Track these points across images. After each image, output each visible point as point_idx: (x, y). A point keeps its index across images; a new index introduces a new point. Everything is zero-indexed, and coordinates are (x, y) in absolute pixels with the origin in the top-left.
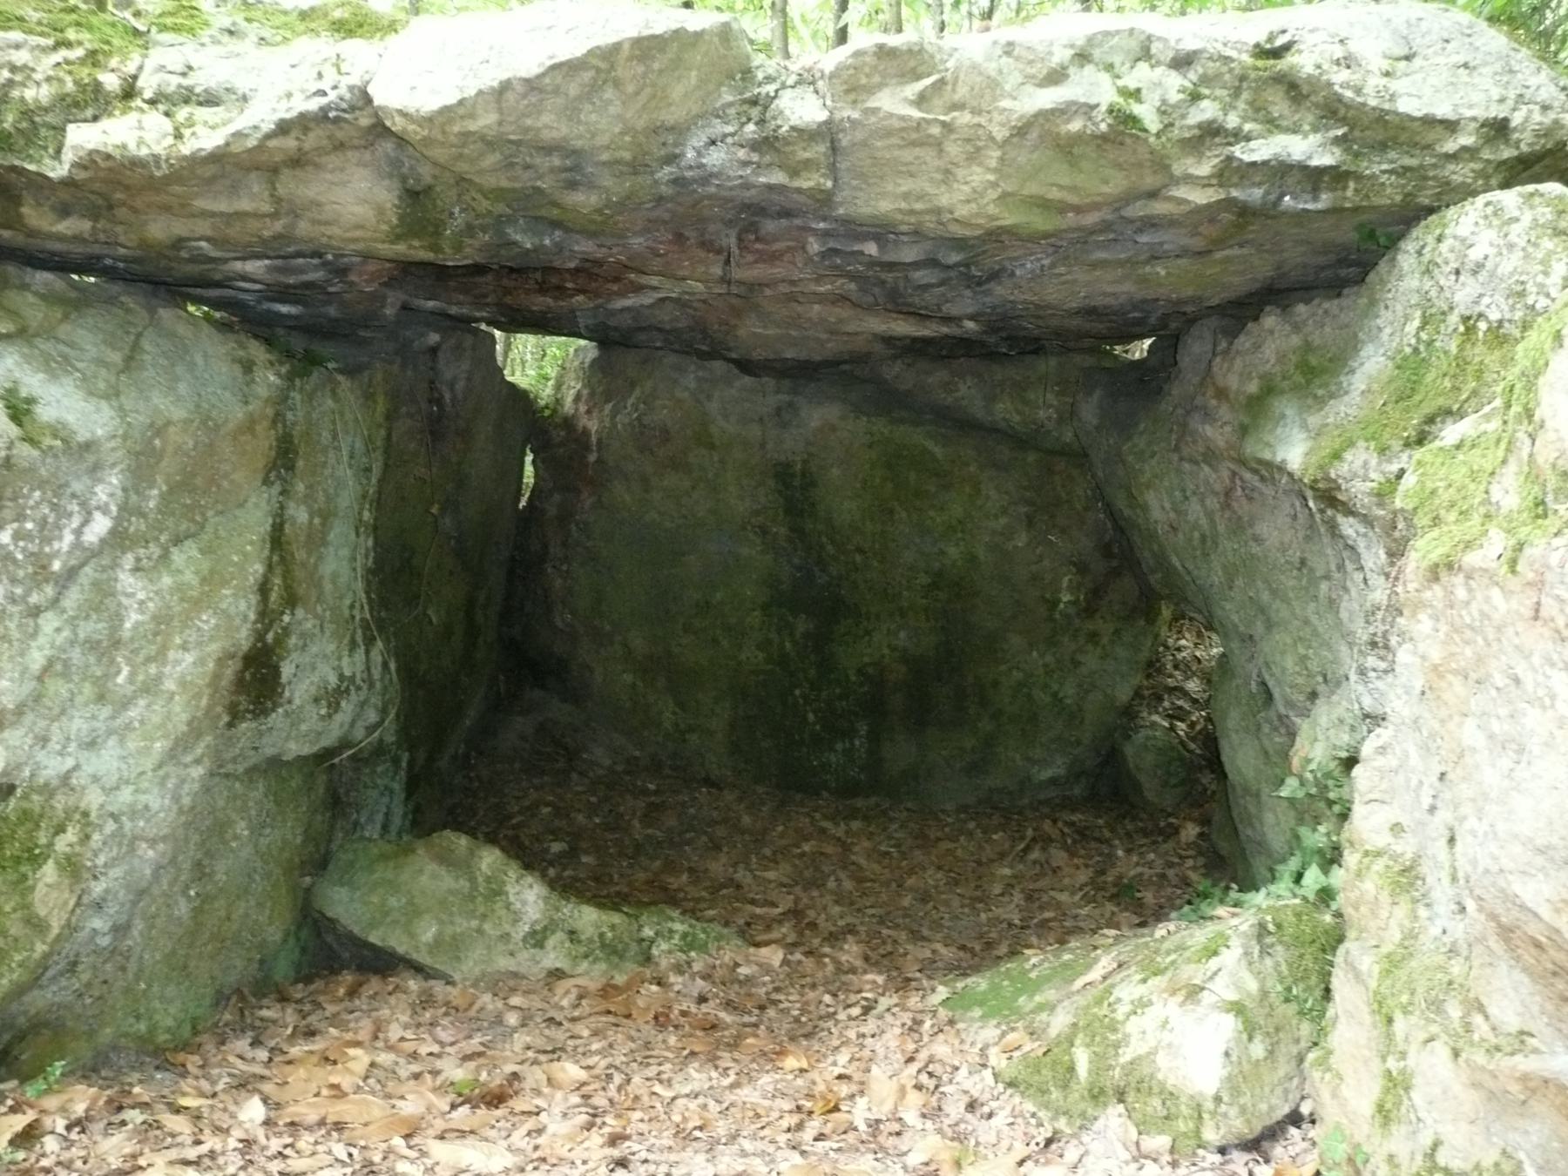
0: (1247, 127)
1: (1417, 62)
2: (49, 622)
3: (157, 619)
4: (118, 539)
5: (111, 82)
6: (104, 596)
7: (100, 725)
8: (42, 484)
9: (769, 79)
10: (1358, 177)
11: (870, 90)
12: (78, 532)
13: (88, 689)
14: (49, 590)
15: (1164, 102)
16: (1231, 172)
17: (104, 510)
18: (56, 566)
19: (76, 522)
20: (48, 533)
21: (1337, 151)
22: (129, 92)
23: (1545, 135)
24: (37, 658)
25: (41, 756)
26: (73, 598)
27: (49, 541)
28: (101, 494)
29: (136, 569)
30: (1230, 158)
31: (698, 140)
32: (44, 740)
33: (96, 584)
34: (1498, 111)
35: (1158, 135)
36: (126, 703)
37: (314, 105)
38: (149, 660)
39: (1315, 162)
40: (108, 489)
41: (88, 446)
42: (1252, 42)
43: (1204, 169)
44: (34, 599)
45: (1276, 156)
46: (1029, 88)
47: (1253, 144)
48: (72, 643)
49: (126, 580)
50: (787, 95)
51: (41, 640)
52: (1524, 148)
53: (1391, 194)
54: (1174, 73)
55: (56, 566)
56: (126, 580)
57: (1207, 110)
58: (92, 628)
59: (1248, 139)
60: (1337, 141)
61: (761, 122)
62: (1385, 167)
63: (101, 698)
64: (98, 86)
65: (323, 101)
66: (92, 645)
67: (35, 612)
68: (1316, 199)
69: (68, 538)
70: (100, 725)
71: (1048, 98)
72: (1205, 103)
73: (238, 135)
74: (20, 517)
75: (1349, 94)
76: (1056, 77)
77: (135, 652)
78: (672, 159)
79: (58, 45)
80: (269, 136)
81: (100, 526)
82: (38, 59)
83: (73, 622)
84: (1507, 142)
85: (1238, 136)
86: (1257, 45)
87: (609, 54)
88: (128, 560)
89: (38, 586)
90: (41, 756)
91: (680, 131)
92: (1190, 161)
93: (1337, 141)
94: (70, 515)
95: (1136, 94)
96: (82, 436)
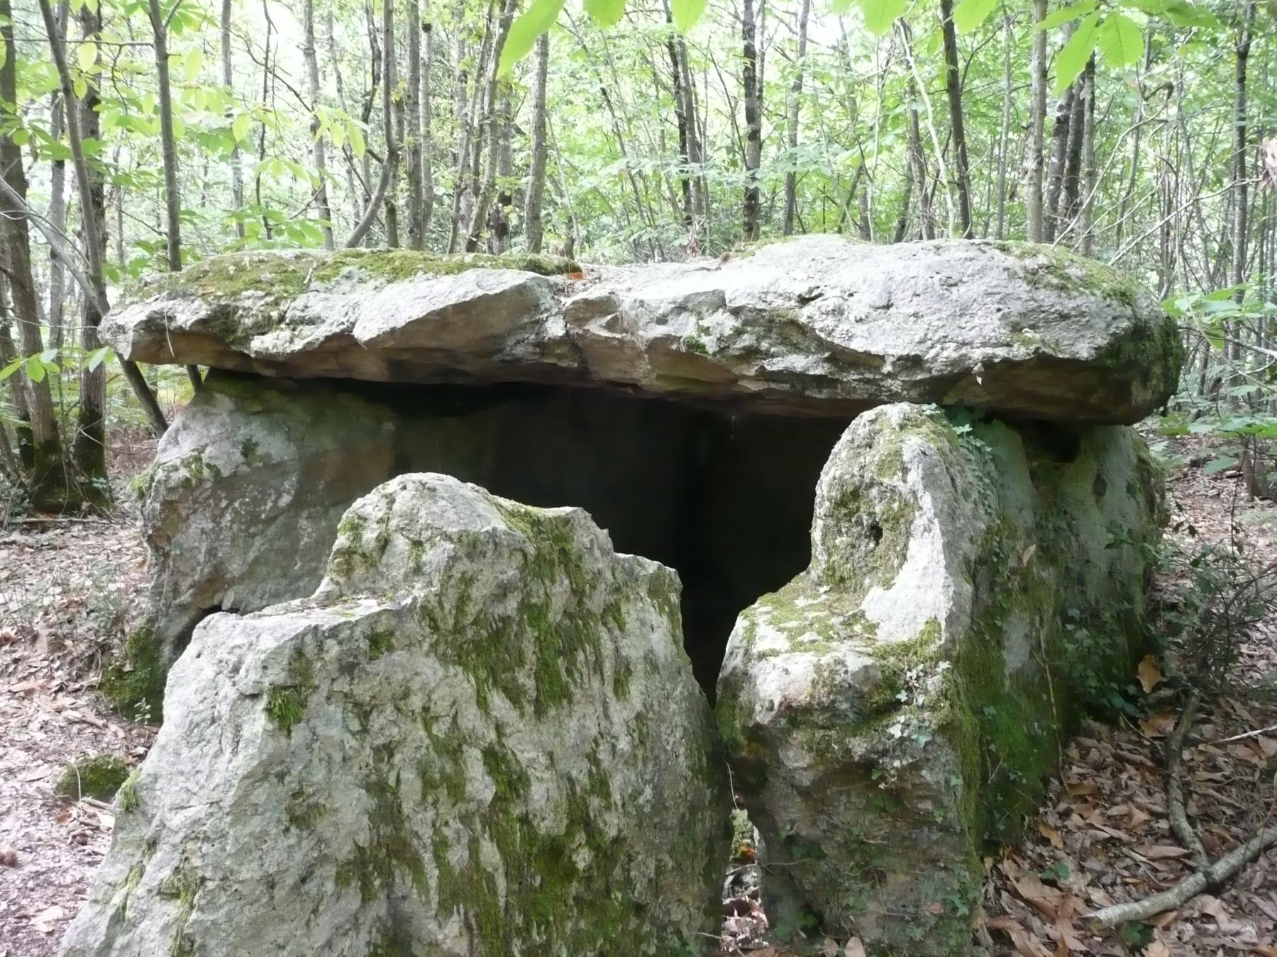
0: (773, 349)
1: (892, 310)
2: (258, 541)
3: (317, 541)
4: (298, 504)
5: (275, 314)
6: (290, 531)
7: (282, 588)
8: (254, 483)
9: (547, 310)
10: (842, 382)
11: (587, 320)
12: (275, 502)
13: (278, 571)
14: (260, 527)
15: (722, 335)
16: (764, 375)
17: (288, 493)
18: (263, 516)
19: (273, 498)
20: (257, 502)
21: (826, 365)
22: (282, 319)
23: (952, 365)
24: (251, 556)
25: (251, 598)
26: (272, 530)
27: (259, 506)
28: (287, 485)
29: (307, 518)
30: (762, 367)
31: (510, 342)
32: (254, 592)
33: (284, 525)
34: (913, 351)
35: (714, 354)
36: (298, 578)
37: (337, 330)
38: (312, 560)
39: (811, 373)
40: (290, 483)
41: (279, 465)
42: (797, 293)
43: (752, 372)
44: (252, 530)
45: (786, 369)
46: (653, 325)
47: (775, 360)
48: (271, 550)
49: (303, 523)
50: (551, 319)
51: (254, 548)
52: (934, 373)
53: (861, 393)
54: (732, 317)
55: (263, 516)
56: (303, 523)
57: (747, 340)
58: (283, 543)
59: (773, 356)
60: (827, 360)
61: (538, 334)
62: (856, 377)
63: (284, 576)
64: (270, 317)
65: (342, 327)
66: (280, 552)
67: (253, 536)
68: (820, 392)
69: (270, 504)
70: (282, 588)
71: (659, 331)
72: (746, 336)
73: (309, 343)
74: (244, 496)
75: (823, 335)
76: (662, 321)
77: (305, 556)
78: (500, 351)
79: (267, 295)
80: (322, 343)
81: (286, 500)
82: (254, 304)
83: (271, 541)
84: (922, 369)
85: (768, 355)
86: (800, 296)
87: (442, 313)
88: (305, 514)
89: (255, 525)
90: (251, 598)
91: (501, 338)
92: (745, 366)
93: (827, 360)
94: (270, 495)
95: (706, 331)
96: (276, 459)
